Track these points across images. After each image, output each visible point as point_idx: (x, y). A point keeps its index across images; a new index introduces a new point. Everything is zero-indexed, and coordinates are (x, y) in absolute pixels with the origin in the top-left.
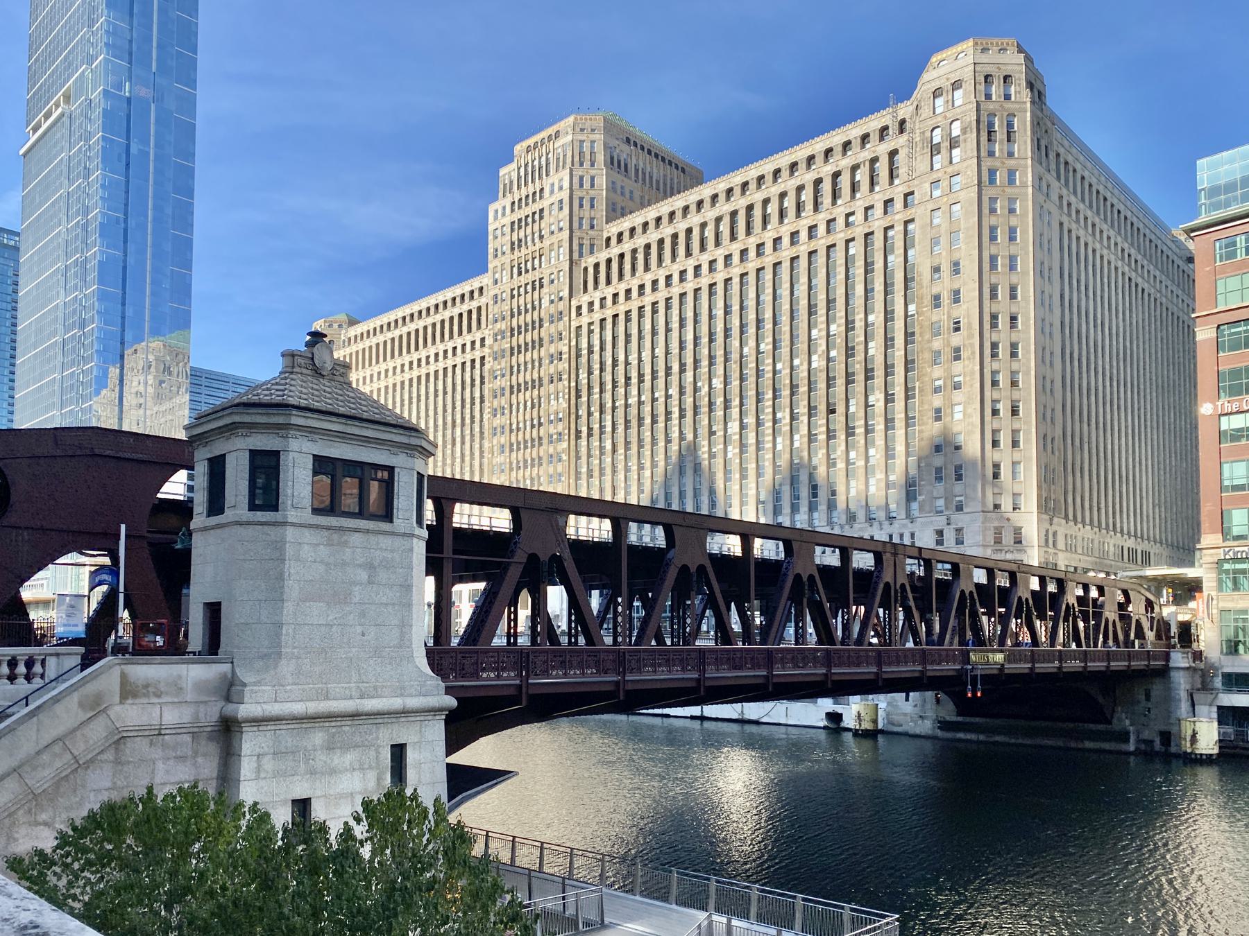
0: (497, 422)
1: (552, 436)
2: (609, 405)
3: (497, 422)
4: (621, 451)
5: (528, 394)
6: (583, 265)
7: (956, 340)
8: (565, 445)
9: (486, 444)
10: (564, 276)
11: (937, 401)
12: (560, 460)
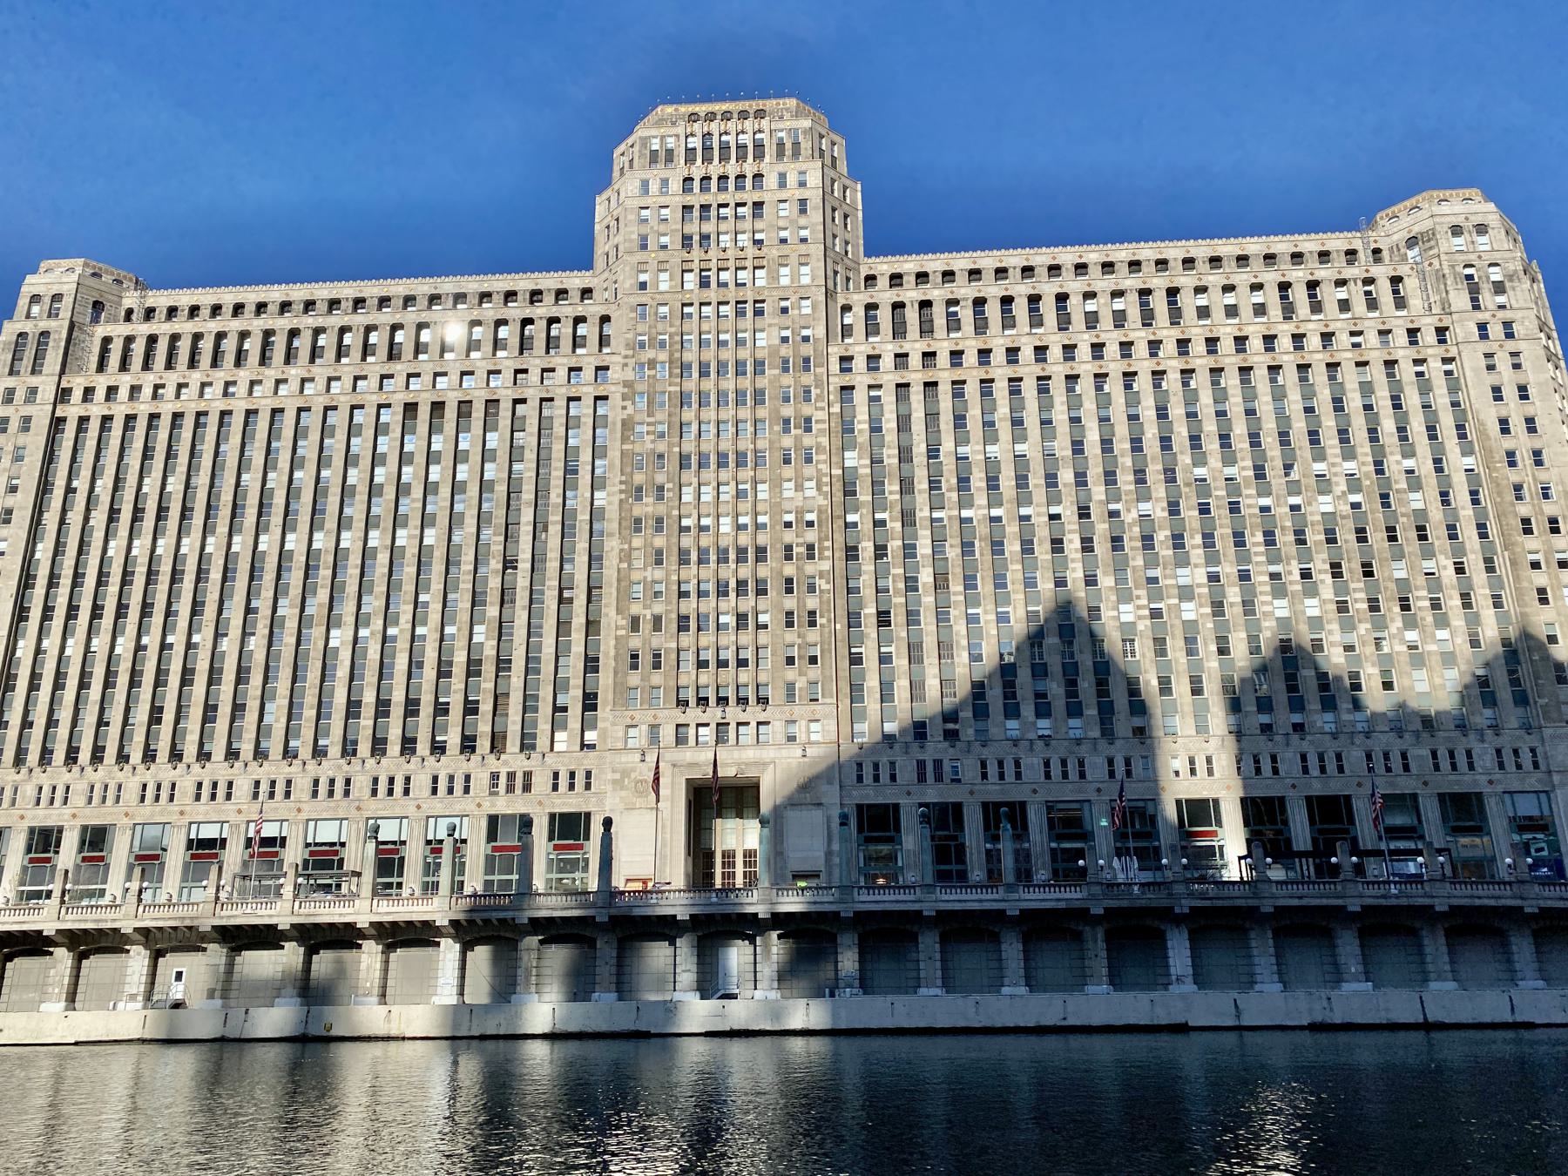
0: (647, 507)
1: (789, 548)
2: (923, 513)
3: (647, 507)
4: (956, 587)
5: (725, 475)
6: (841, 301)
7: (1550, 509)
8: (826, 566)
9: (612, 546)
10: (814, 307)
11: (1540, 579)
12: (811, 589)
